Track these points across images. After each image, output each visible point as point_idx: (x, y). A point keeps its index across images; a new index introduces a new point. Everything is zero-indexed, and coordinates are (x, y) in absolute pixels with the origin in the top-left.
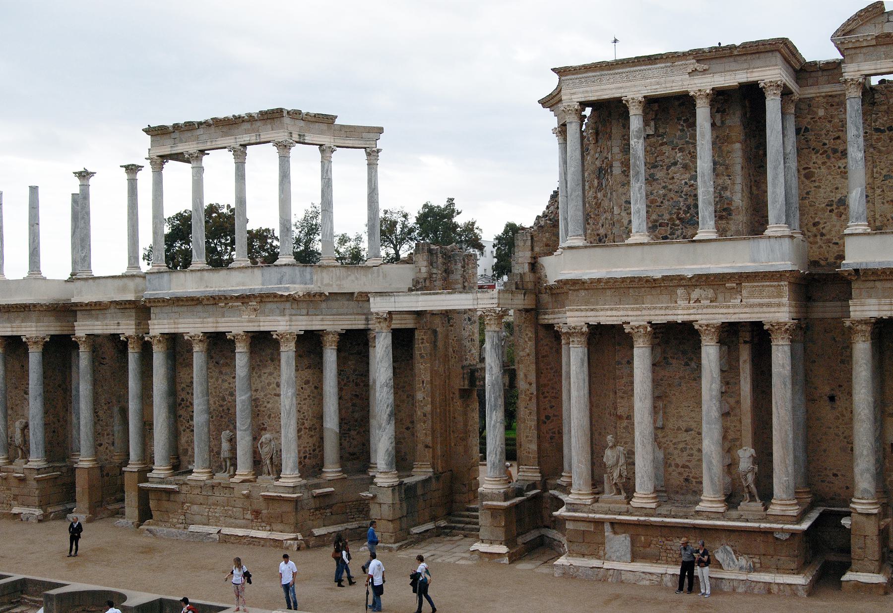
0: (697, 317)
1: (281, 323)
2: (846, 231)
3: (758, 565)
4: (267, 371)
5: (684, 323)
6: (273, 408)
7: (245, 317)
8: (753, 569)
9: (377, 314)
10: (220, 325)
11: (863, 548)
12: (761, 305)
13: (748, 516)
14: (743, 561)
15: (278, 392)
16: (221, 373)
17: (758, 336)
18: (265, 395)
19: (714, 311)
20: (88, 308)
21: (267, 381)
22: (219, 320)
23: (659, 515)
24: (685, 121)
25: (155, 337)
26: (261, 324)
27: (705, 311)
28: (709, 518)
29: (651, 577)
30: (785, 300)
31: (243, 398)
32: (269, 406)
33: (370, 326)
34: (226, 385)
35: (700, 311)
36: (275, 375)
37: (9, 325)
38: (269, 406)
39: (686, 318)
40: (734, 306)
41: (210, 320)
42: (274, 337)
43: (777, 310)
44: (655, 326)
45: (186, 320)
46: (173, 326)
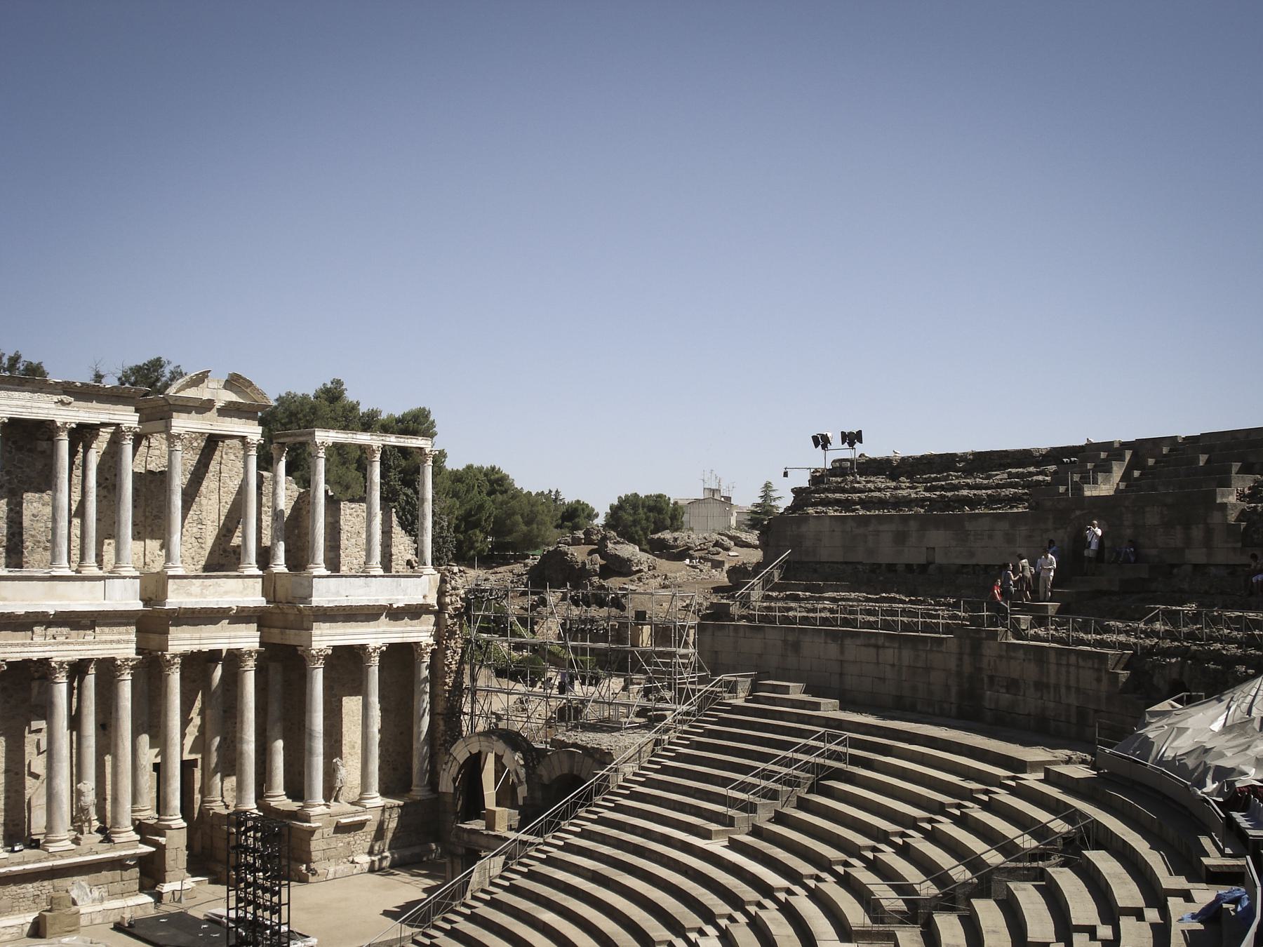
0: (53, 654)
2: (170, 573)
3: (105, 895)
5: (39, 660)
8: (102, 900)
11: (175, 860)
12: (112, 642)
13: (93, 849)
14: (96, 893)
17: (108, 669)
19: (71, 647)
23: (13, 864)
24: (14, 443)
27: (61, 648)
28: (62, 857)
29: (12, 930)
30: (133, 637)
35: (55, 648)
39: (42, 655)
40: (89, 643)
43: (121, 645)
44: (8, 663)
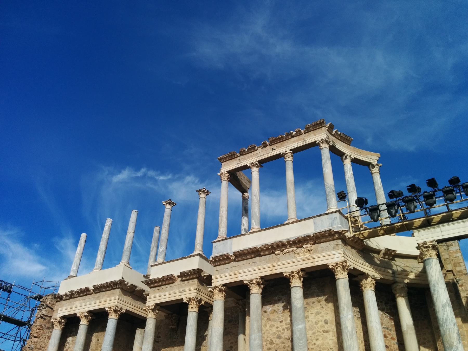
1: (336, 256)
4: (315, 311)
6: (323, 344)
7: (300, 257)
9: (425, 243)
10: (276, 268)
15: (326, 329)
16: (269, 319)
18: (314, 333)
20: (160, 284)
21: (314, 321)
22: (276, 264)
25: (216, 287)
26: (316, 260)
31: (300, 327)
32: (318, 343)
33: (397, 279)
34: (274, 329)
36: (323, 314)
37: (97, 301)
38: (318, 343)
41: (267, 265)
42: (331, 267)
45: (246, 270)
46: (233, 276)
